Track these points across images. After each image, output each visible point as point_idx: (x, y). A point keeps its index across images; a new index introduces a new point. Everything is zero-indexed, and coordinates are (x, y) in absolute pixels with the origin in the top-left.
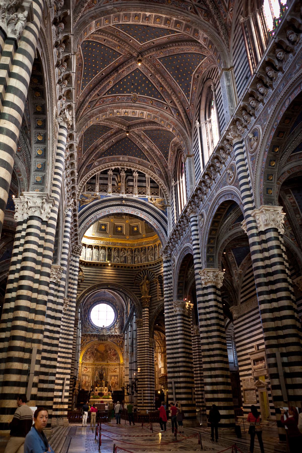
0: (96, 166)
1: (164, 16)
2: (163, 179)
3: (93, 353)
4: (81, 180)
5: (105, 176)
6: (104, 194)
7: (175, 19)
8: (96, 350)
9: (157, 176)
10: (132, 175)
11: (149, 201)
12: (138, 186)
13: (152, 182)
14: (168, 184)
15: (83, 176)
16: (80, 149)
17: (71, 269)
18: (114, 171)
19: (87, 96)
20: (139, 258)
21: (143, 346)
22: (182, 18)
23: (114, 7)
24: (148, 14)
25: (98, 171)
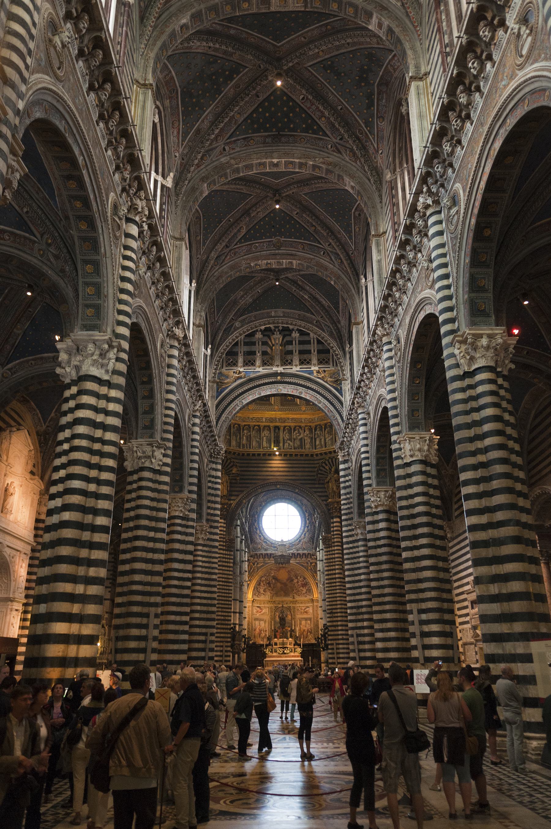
0: (238, 328)
1: (297, 161)
2: (335, 340)
3: (269, 583)
4: (217, 351)
5: (253, 339)
6: (250, 369)
7: (311, 163)
8: (274, 578)
9: (326, 335)
10: (290, 335)
11: (315, 374)
12: (301, 352)
13: (319, 342)
14: (342, 347)
15: (220, 345)
16: (213, 310)
17: (210, 481)
18: (263, 332)
19: (211, 252)
20: (323, 440)
21: (334, 576)
22: (321, 160)
23: (231, 158)
24: (275, 161)
25: (241, 335)
